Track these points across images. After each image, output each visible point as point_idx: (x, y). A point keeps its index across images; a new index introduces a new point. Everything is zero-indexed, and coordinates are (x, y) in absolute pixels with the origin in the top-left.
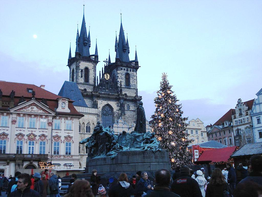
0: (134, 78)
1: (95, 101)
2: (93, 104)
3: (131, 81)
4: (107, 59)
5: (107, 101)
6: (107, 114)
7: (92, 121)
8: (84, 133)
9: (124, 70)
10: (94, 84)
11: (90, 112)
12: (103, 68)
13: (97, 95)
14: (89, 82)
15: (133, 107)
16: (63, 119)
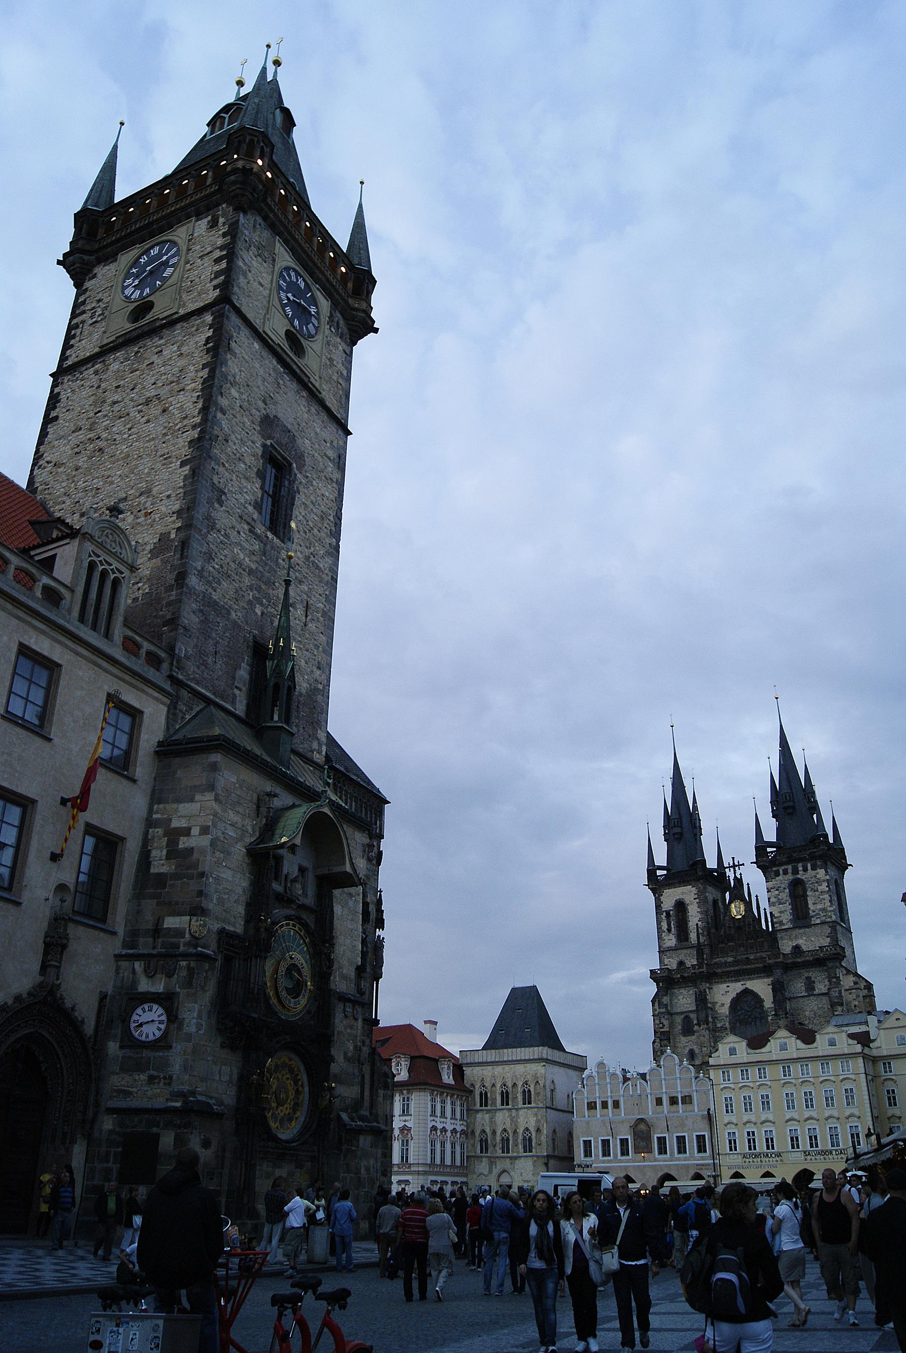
1: (700, 992)
3: (810, 902)
7: (535, 1076)
9: (785, 872)
16: (397, 1095)
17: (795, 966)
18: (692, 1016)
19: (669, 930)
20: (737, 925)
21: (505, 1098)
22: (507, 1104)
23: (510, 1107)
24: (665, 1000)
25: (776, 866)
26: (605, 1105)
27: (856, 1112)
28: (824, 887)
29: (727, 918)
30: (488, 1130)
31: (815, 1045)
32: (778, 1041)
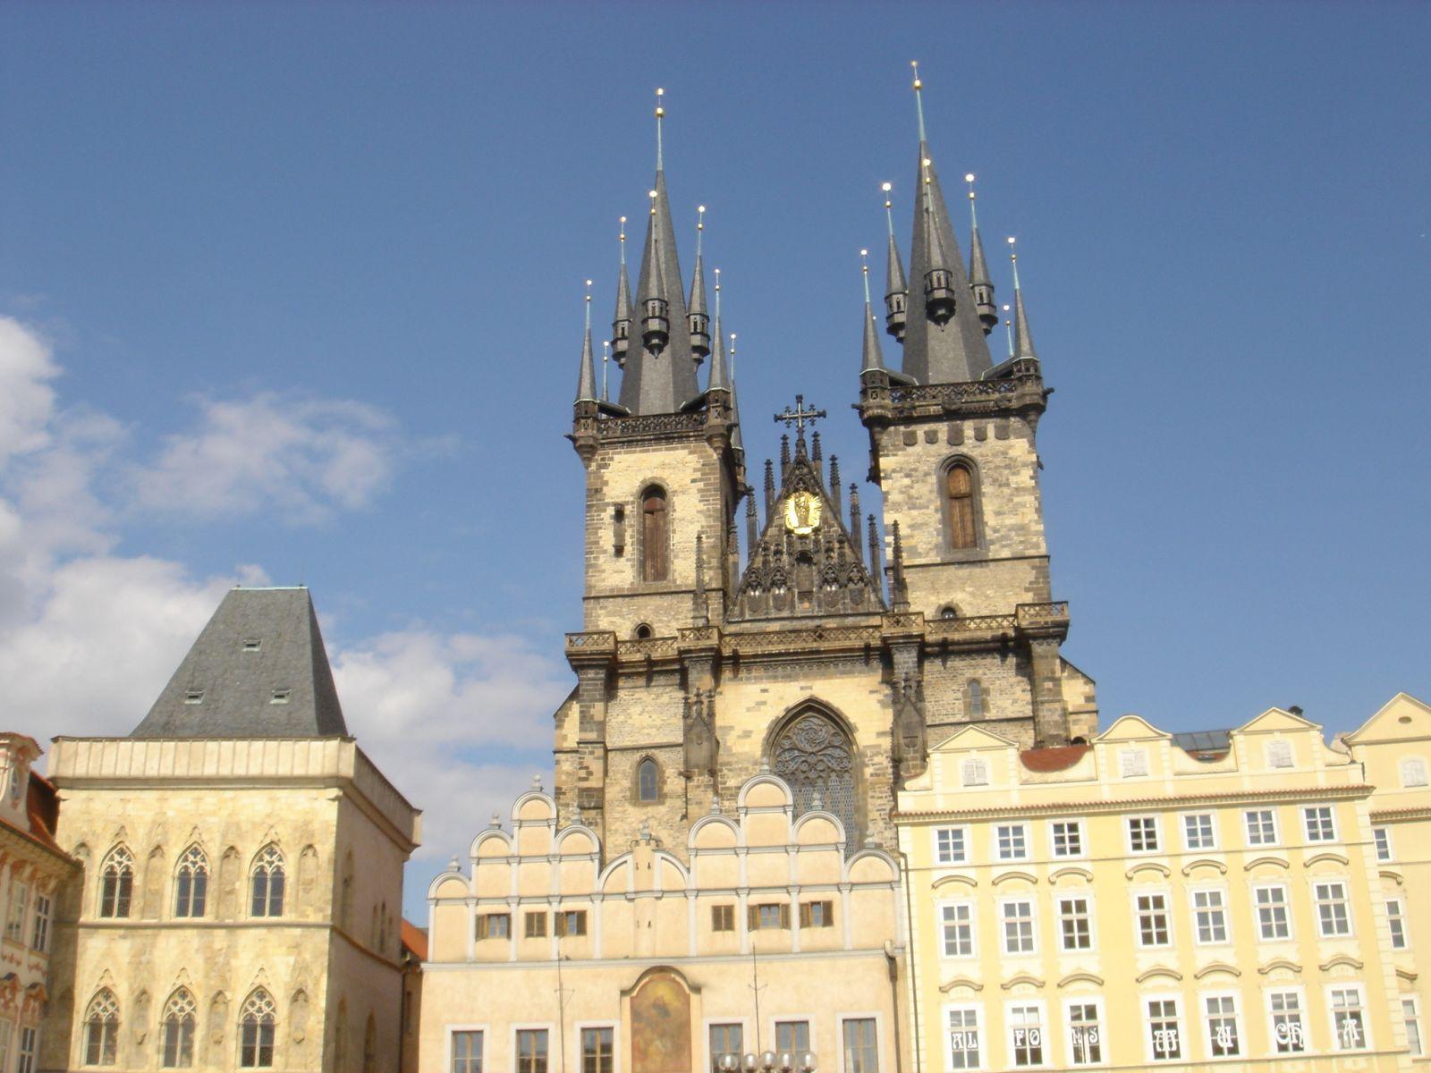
0: (1014, 480)
1: (698, 695)
2: (686, 717)
3: (988, 507)
4: (799, 399)
5: (803, 683)
6: (812, 775)
7: (304, 829)
8: (228, 921)
9: (931, 439)
10: (699, 581)
11: (284, 771)
12: (768, 463)
13: (711, 649)
14: (670, 577)
15: (1018, 690)
17: (945, 650)
18: (661, 756)
19: (619, 551)
20: (798, 547)
21: (193, 891)
22: (199, 910)
23: (207, 918)
24: (598, 709)
25: (910, 420)
26: (535, 925)
27: (1352, 951)
28: (1025, 477)
29: (772, 531)
30: (123, 992)
31: (1228, 762)
32: (1119, 747)
